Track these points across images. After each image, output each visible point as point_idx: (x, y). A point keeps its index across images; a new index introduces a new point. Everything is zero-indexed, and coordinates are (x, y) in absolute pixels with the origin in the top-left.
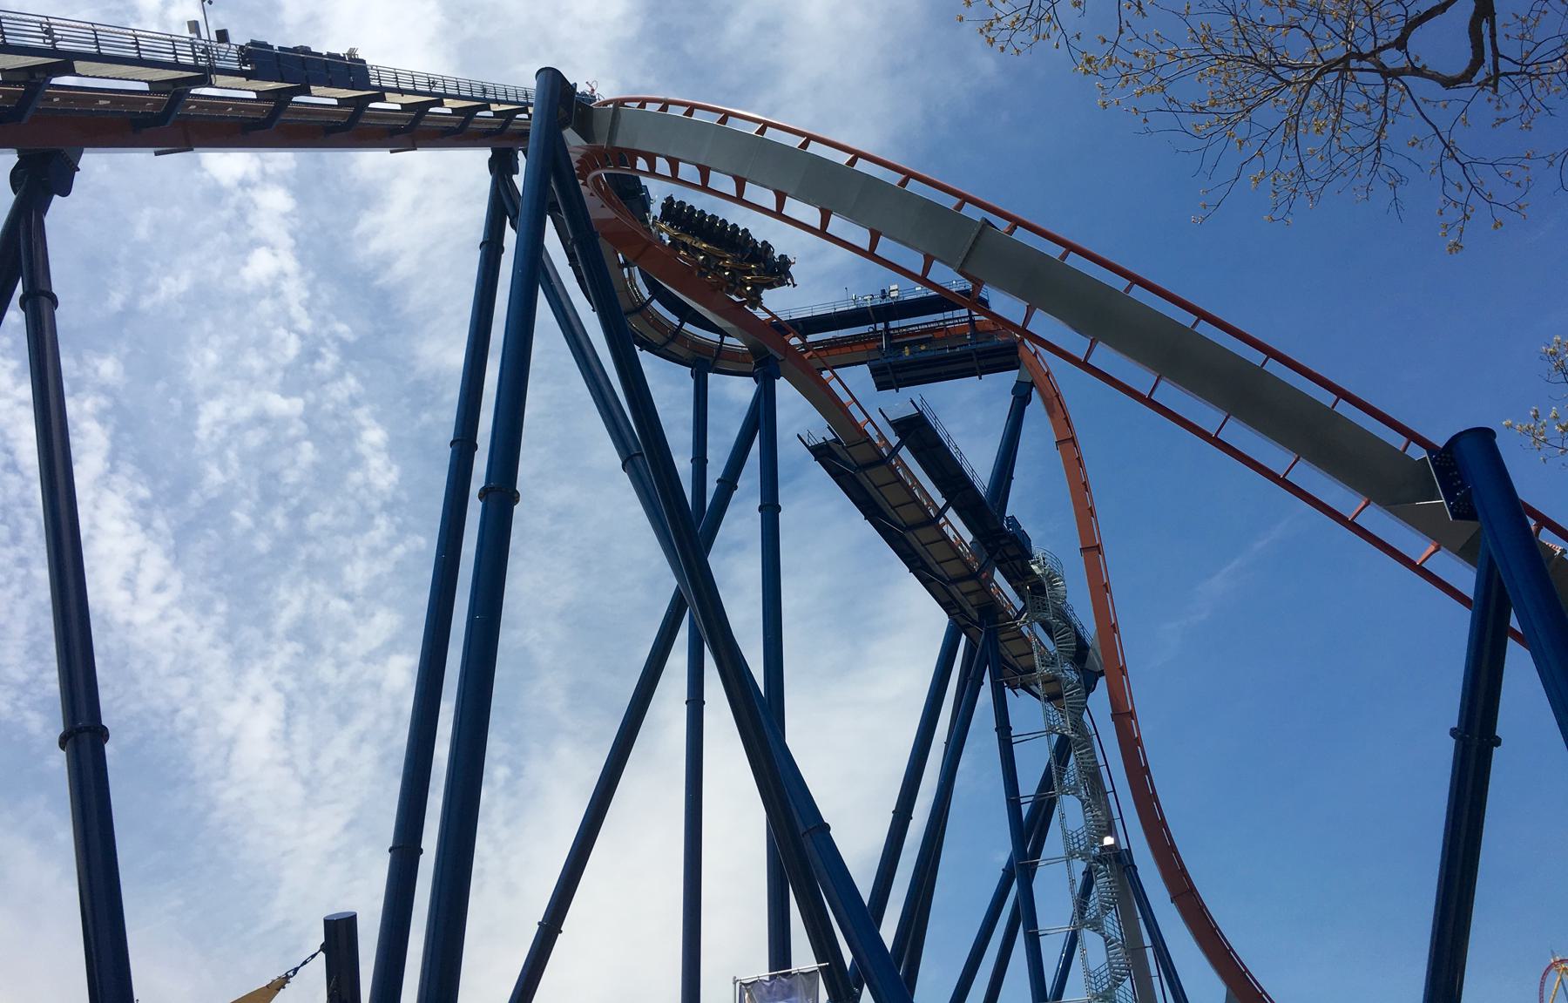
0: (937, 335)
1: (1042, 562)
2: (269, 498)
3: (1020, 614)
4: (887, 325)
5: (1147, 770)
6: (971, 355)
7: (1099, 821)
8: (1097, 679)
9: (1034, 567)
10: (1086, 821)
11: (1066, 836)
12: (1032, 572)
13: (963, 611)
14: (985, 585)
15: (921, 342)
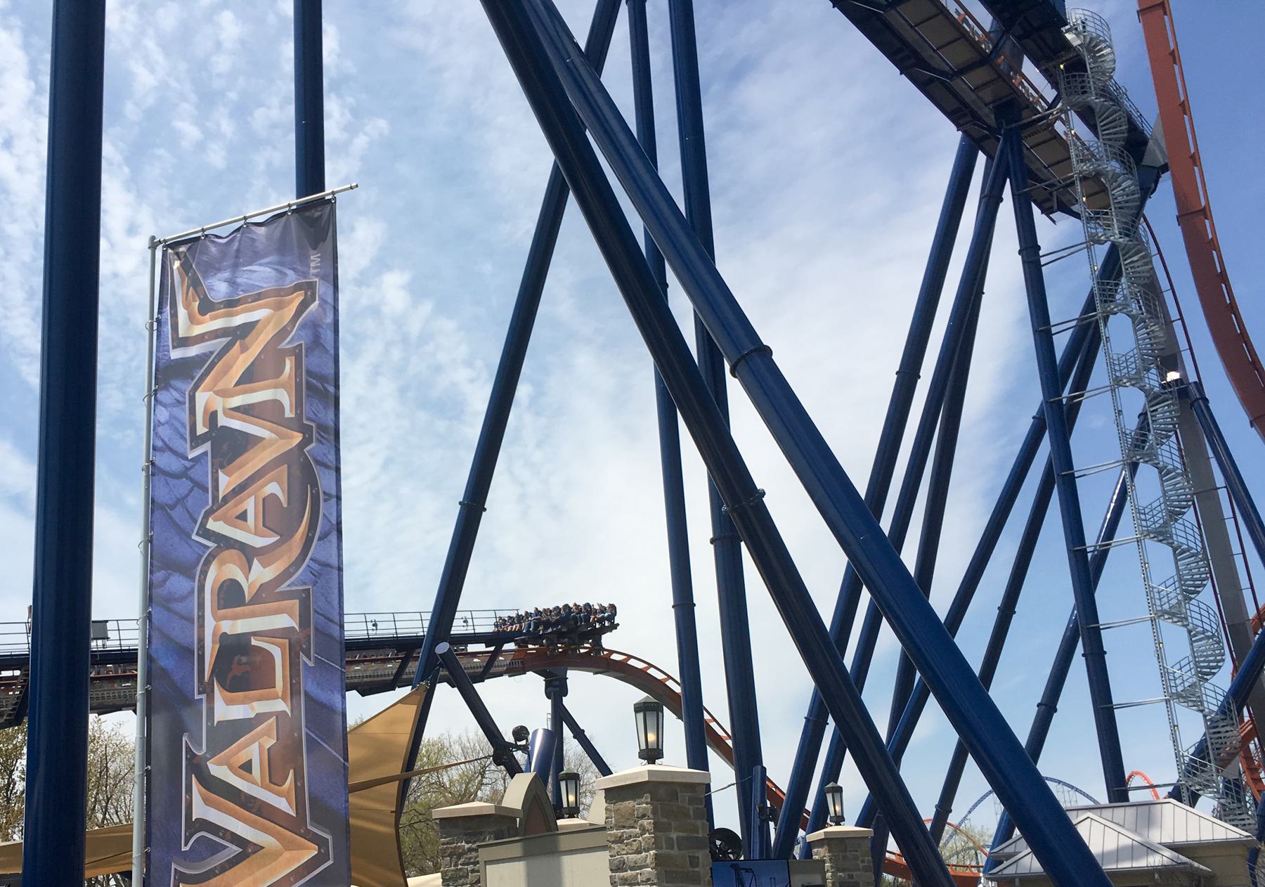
1: (1080, 28)
2: (207, 99)
3: (1052, 106)
5: (1223, 277)
7: (1155, 338)
8: (1158, 177)
10: (1138, 340)
11: (1111, 364)
12: (1067, 45)
13: (976, 117)
14: (1006, 79)
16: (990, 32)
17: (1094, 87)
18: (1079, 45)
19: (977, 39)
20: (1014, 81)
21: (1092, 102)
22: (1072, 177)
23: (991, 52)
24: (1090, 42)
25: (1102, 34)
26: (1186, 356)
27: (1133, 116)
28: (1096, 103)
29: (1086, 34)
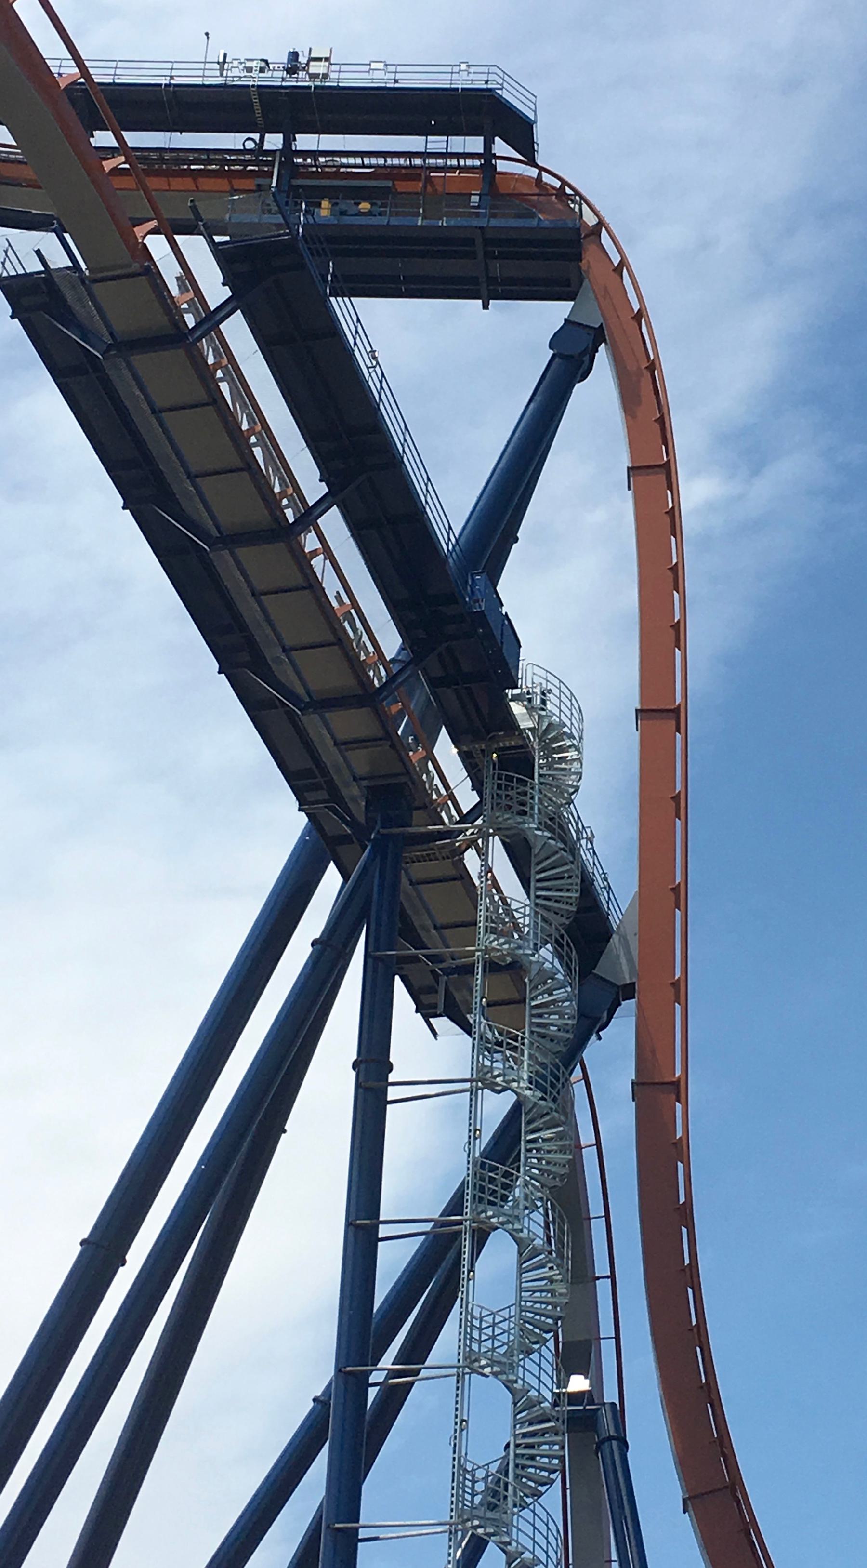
0: (402, 186)
1: (537, 701)
4: (288, 141)
6: (471, 242)
9: (517, 709)
10: (521, 1290)
11: (466, 1325)
15: (359, 194)
16: (393, 661)
17: (539, 809)
18: (529, 729)
19: (363, 657)
20: (411, 753)
21: (529, 833)
22: (472, 954)
23: (383, 687)
24: (546, 731)
25: (568, 723)
26: (607, 1348)
27: (596, 883)
28: (536, 835)
29: (543, 713)
